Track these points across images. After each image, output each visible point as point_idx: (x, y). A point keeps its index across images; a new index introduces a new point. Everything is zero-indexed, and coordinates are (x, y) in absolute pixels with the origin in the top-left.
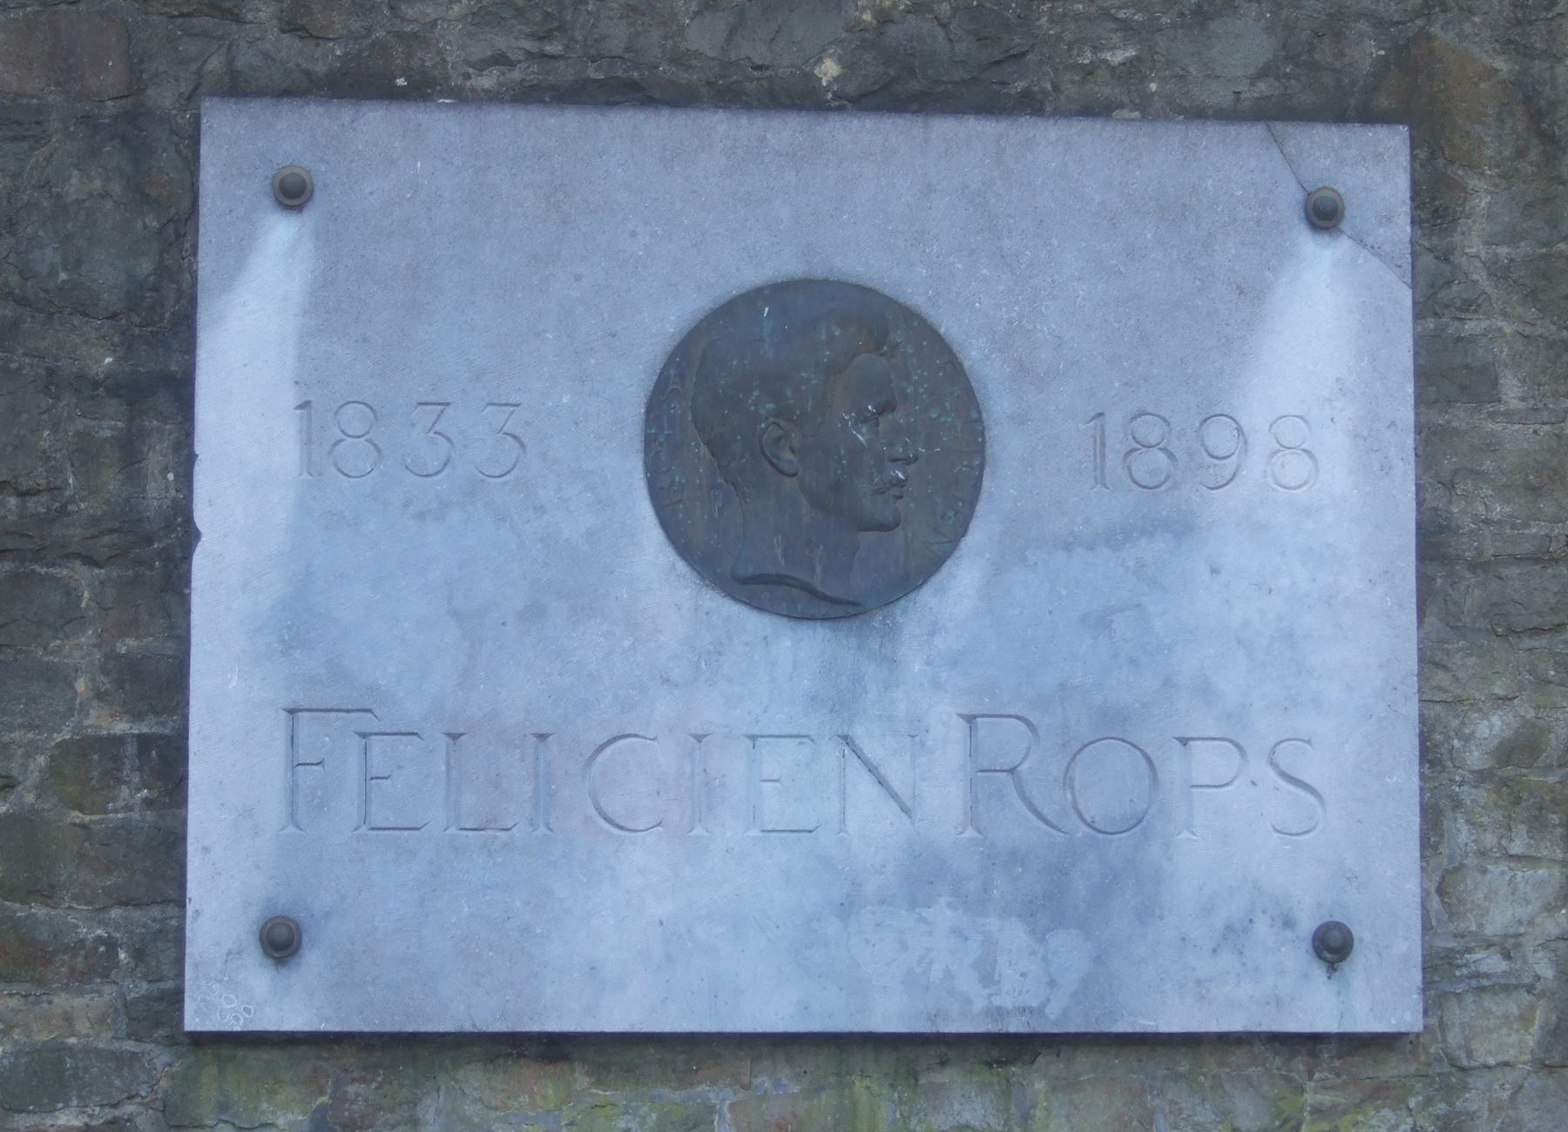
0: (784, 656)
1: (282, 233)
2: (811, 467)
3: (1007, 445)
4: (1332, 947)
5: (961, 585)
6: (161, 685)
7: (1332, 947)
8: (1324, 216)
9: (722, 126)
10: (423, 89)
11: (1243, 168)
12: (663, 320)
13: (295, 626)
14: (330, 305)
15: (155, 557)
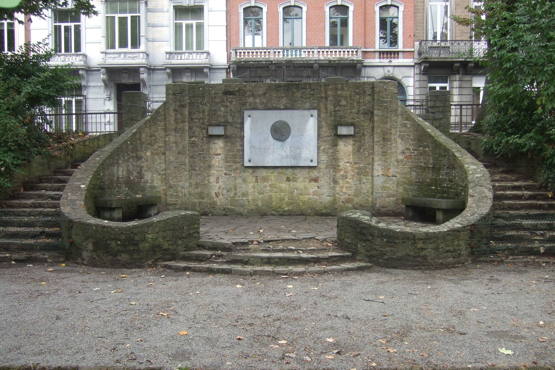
0: (279, 143)
1: (249, 119)
2: (280, 132)
3: (292, 130)
4: (312, 161)
5: (289, 139)
6: (243, 146)
7: (312, 161)
8: (312, 116)
9: (275, 111)
10: (258, 109)
11: (307, 113)
12: (272, 123)
13: (250, 142)
14: (252, 123)
15: (242, 138)
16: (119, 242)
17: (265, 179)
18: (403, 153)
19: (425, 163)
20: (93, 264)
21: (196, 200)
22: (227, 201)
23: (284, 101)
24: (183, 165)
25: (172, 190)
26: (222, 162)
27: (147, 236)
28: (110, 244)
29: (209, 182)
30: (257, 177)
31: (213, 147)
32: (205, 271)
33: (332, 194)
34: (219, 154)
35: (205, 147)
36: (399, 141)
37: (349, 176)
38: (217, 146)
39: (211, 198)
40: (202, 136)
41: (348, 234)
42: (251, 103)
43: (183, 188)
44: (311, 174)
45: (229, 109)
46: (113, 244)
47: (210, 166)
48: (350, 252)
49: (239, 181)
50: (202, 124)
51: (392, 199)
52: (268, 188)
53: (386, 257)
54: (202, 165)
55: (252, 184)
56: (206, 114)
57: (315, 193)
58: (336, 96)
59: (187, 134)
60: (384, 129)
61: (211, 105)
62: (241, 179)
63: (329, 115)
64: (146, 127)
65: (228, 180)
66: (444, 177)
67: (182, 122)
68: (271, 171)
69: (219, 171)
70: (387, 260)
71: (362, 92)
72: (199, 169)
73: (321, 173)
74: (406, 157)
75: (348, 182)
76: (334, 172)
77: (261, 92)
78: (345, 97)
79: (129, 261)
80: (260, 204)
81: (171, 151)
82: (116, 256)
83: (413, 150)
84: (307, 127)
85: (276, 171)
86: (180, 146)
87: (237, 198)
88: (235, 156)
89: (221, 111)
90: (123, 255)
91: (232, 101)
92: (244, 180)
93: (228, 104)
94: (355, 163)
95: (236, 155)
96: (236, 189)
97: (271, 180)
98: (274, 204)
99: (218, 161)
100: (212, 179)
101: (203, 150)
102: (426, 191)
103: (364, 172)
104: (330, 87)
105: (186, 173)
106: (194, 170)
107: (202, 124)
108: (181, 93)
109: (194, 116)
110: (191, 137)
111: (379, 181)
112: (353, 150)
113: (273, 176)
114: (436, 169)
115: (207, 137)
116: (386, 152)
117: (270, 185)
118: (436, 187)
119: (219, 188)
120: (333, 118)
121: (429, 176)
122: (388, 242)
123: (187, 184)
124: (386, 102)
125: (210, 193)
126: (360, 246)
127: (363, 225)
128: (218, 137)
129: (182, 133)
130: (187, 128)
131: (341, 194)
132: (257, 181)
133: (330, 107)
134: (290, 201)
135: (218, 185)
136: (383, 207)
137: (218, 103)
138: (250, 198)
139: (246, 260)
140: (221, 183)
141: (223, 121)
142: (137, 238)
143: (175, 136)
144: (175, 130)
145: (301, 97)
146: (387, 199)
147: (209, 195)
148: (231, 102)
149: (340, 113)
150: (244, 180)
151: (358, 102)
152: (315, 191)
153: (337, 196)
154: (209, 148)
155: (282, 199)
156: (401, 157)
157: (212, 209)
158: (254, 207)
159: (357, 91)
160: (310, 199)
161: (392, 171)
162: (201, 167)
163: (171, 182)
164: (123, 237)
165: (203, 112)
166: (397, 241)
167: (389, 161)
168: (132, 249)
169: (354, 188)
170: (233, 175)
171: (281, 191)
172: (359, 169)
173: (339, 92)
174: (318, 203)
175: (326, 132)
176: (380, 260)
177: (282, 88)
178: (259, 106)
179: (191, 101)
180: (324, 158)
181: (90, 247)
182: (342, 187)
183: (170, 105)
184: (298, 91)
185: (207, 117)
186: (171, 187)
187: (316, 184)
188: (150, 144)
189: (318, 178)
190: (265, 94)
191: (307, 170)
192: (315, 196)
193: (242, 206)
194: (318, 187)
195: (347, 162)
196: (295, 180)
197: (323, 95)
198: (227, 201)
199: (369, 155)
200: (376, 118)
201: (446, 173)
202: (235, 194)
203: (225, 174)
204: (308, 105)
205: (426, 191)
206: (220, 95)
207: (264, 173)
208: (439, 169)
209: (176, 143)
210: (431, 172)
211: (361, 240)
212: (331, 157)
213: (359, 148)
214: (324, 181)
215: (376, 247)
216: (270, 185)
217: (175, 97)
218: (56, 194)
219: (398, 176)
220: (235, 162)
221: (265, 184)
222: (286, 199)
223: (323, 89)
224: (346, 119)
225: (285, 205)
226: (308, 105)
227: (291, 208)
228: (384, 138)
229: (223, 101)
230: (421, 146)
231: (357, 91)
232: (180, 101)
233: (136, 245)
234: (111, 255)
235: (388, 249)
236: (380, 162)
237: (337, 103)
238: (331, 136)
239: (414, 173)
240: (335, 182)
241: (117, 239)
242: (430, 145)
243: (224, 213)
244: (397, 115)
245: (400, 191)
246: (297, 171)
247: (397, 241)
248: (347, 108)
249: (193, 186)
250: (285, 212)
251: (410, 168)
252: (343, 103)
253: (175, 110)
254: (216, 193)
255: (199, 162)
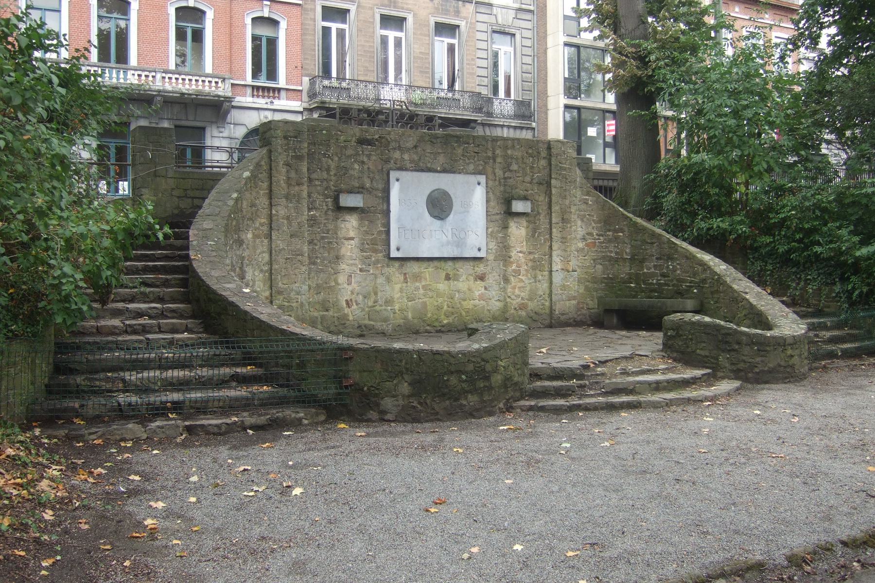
0: (438, 223)
1: (397, 183)
2: (439, 206)
3: (454, 204)
4: (479, 250)
5: (451, 216)
6: (387, 225)
7: (479, 250)
8: (479, 184)
9: (431, 174)
10: (406, 170)
11: (473, 179)
12: (428, 192)
13: (399, 220)
14: (401, 190)
15: (387, 213)
16: (463, 377)
17: (417, 277)
18: (584, 239)
19: (617, 253)
20: (410, 416)
21: (316, 314)
22: (364, 313)
23: (441, 159)
24: (298, 255)
25: (281, 297)
26: (356, 250)
27: (500, 363)
28: (448, 380)
29: (337, 284)
30: (405, 274)
31: (343, 226)
32: (602, 409)
33: (502, 298)
34: (352, 239)
35: (331, 227)
36: (579, 223)
37: (523, 272)
38: (348, 225)
39: (340, 310)
40: (325, 207)
41: (704, 345)
42: (397, 159)
43: (298, 293)
44: (477, 269)
45: (366, 167)
46: (453, 380)
47: (338, 258)
48: (707, 368)
49: (381, 280)
50: (326, 189)
51: (574, 302)
52: (421, 291)
53: (757, 370)
54: (326, 255)
55: (399, 286)
56: (332, 173)
57: (481, 297)
58: (506, 157)
59: (305, 203)
60: (563, 206)
61: (340, 158)
62: (384, 278)
63: (497, 183)
64: (247, 190)
65: (366, 279)
66: (653, 270)
67: (298, 184)
68: (425, 264)
69: (352, 265)
70: (758, 373)
71: (535, 153)
72: (322, 262)
73: (489, 268)
74: (587, 245)
75: (522, 281)
76: (504, 266)
77: (410, 145)
78: (517, 159)
79: (477, 406)
80: (410, 316)
81: (280, 231)
82: (457, 400)
83: (597, 235)
84: (473, 197)
85: (432, 264)
86: (295, 224)
87: (378, 308)
88: (374, 242)
89: (354, 169)
90: (470, 396)
91: (370, 154)
92: (388, 280)
93: (365, 159)
94: (530, 253)
95: (378, 241)
96: (376, 294)
97: (426, 279)
98: (429, 315)
99: (349, 250)
100: (342, 279)
101: (328, 231)
102: (620, 290)
103: (541, 264)
104: (498, 143)
105: (304, 269)
106: (314, 263)
107: (326, 189)
108: (296, 137)
109: (314, 176)
110: (310, 210)
111: (558, 278)
112: (527, 235)
113: (427, 271)
114: (637, 259)
115: (333, 211)
116: (566, 238)
117: (423, 287)
118: (637, 284)
119: (352, 293)
120: (502, 188)
121: (624, 271)
122: (759, 350)
123: (305, 287)
124: (565, 169)
125: (338, 300)
126: (723, 359)
127: (726, 331)
128: (351, 210)
129: (298, 201)
130: (305, 194)
131: (513, 297)
132: (406, 281)
133: (499, 173)
134: (450, 309)
135: (350, 288)
136: (563, 314)
137: (349, 157)
138: (397, 307)
139: (631, 387)
140: (354, 285)
141: (357, 185)
142: (488, 367)
143: (287, 207)
144: (287, 197)
145: (463, 155)
146: (567, 303)
147: (336, 304)
148: (369, 156)
149: (511, 182)
150: (388, 280)
151: (532, 168)
152: (482, 294)
153: (508, 300)
154: (337, 228)
155: (439, 308)
156: (581, 245)
157: (340, 327)
158: (402, 321)
159: (530, 151)
160: (475, 306)
161: (573, 263)
162: (324, 259)
163: (280, 284)
164: (470, 367)
165: (328, 170)
166: (768, 349)
167: (568, 250)
168: (482, 385)
169: (528, 289)
170: (371, 272)
171: (439, 295)
172: (534, 261)
173: (509, 152)
174: (485, 312)
175: (498, 209)
176: (750, 375)
177: (439, 140)
178: (408, 165)
179: (309, 150)
180: (492, 245)
181: (405, 388)
182: (514, 288)
183: (280, 154)
184: (459, 146)
185: (333, 178)
186: (280, 293)
187: (483, 284)
188: (251, 219)
189: (484, 274)
190: (416, 147)
191: (471, 264)
192: (482, 302)
193: (386, 320)
194: (486, 288)
195: (520, 252)
196: (456, 278)
197: (490, 154)
198: (364, 313)
199: (545, 242)
200: (554, 191)
201: (655, 266)
202: (375, 302)
203: (361, 270)
204: (471, 167)
205: (620, 290)
206: (353, 143)
207: (414, 268)
208: (642, 261)
209: (288, 218)
210: (628, 264)
211: (723, 351)
212: (501, 245)
213: (534, 231)
214: (493, 279)
215: (744, 358)
216: (423, 287)
217: (286, 142)
218: (150, 308)
219: (578, 270)
220: (376, 251)
221: (417, 284)
222: (445, 307)
223: (490, 143)
224: (517, 190)
225: (443, 317)
226: (471, 167)
227: (451, 320)
228: (563, 219)
229: (357, 154)
230: (609, 231)
231: (530, 151)
232: (294, 149)
233: (487, 378)
234: (449, 399)
235: (758, 359)
236: (559, 252)
237: (507, 168)
238: (503, 210)
239: (600, 267)
240: (506, 280)
241: (459, 372)
242: (626, 229)
243: (358, 332)
244: (575, 188)
245: (581, 291)
246: (459, 265)
247: (768, 349)
248: (518, 175)
249: (312, 291)
250: (443, 326)
251: (594, 260)
252: (515, 167)
253: (287, 164)
254: (347, 301)
255: (323, 252)
